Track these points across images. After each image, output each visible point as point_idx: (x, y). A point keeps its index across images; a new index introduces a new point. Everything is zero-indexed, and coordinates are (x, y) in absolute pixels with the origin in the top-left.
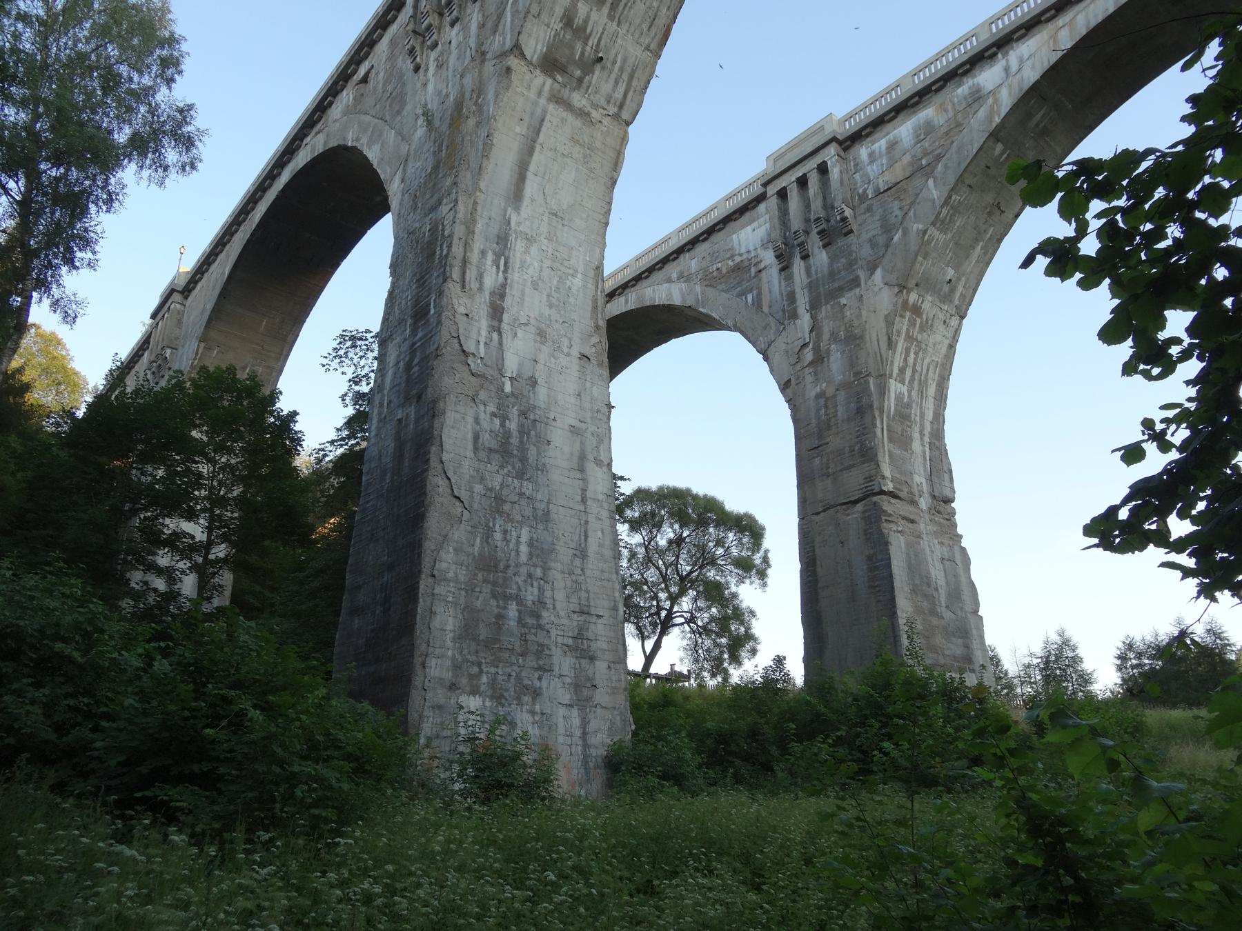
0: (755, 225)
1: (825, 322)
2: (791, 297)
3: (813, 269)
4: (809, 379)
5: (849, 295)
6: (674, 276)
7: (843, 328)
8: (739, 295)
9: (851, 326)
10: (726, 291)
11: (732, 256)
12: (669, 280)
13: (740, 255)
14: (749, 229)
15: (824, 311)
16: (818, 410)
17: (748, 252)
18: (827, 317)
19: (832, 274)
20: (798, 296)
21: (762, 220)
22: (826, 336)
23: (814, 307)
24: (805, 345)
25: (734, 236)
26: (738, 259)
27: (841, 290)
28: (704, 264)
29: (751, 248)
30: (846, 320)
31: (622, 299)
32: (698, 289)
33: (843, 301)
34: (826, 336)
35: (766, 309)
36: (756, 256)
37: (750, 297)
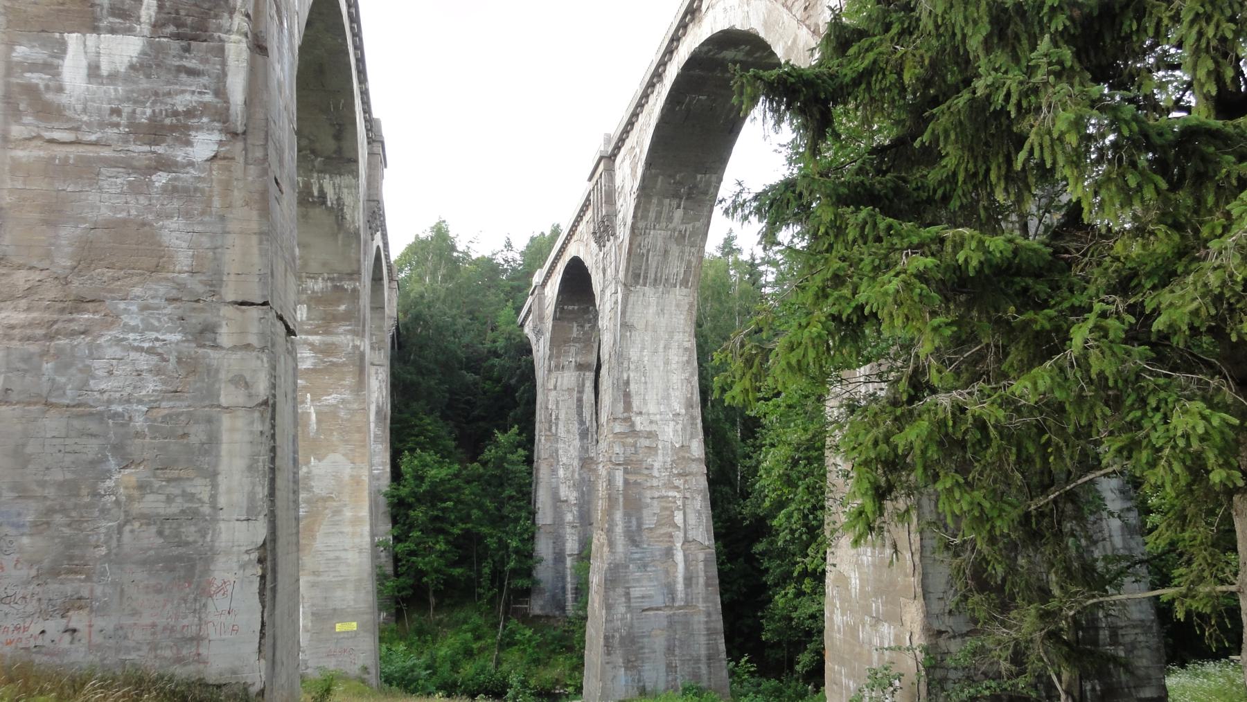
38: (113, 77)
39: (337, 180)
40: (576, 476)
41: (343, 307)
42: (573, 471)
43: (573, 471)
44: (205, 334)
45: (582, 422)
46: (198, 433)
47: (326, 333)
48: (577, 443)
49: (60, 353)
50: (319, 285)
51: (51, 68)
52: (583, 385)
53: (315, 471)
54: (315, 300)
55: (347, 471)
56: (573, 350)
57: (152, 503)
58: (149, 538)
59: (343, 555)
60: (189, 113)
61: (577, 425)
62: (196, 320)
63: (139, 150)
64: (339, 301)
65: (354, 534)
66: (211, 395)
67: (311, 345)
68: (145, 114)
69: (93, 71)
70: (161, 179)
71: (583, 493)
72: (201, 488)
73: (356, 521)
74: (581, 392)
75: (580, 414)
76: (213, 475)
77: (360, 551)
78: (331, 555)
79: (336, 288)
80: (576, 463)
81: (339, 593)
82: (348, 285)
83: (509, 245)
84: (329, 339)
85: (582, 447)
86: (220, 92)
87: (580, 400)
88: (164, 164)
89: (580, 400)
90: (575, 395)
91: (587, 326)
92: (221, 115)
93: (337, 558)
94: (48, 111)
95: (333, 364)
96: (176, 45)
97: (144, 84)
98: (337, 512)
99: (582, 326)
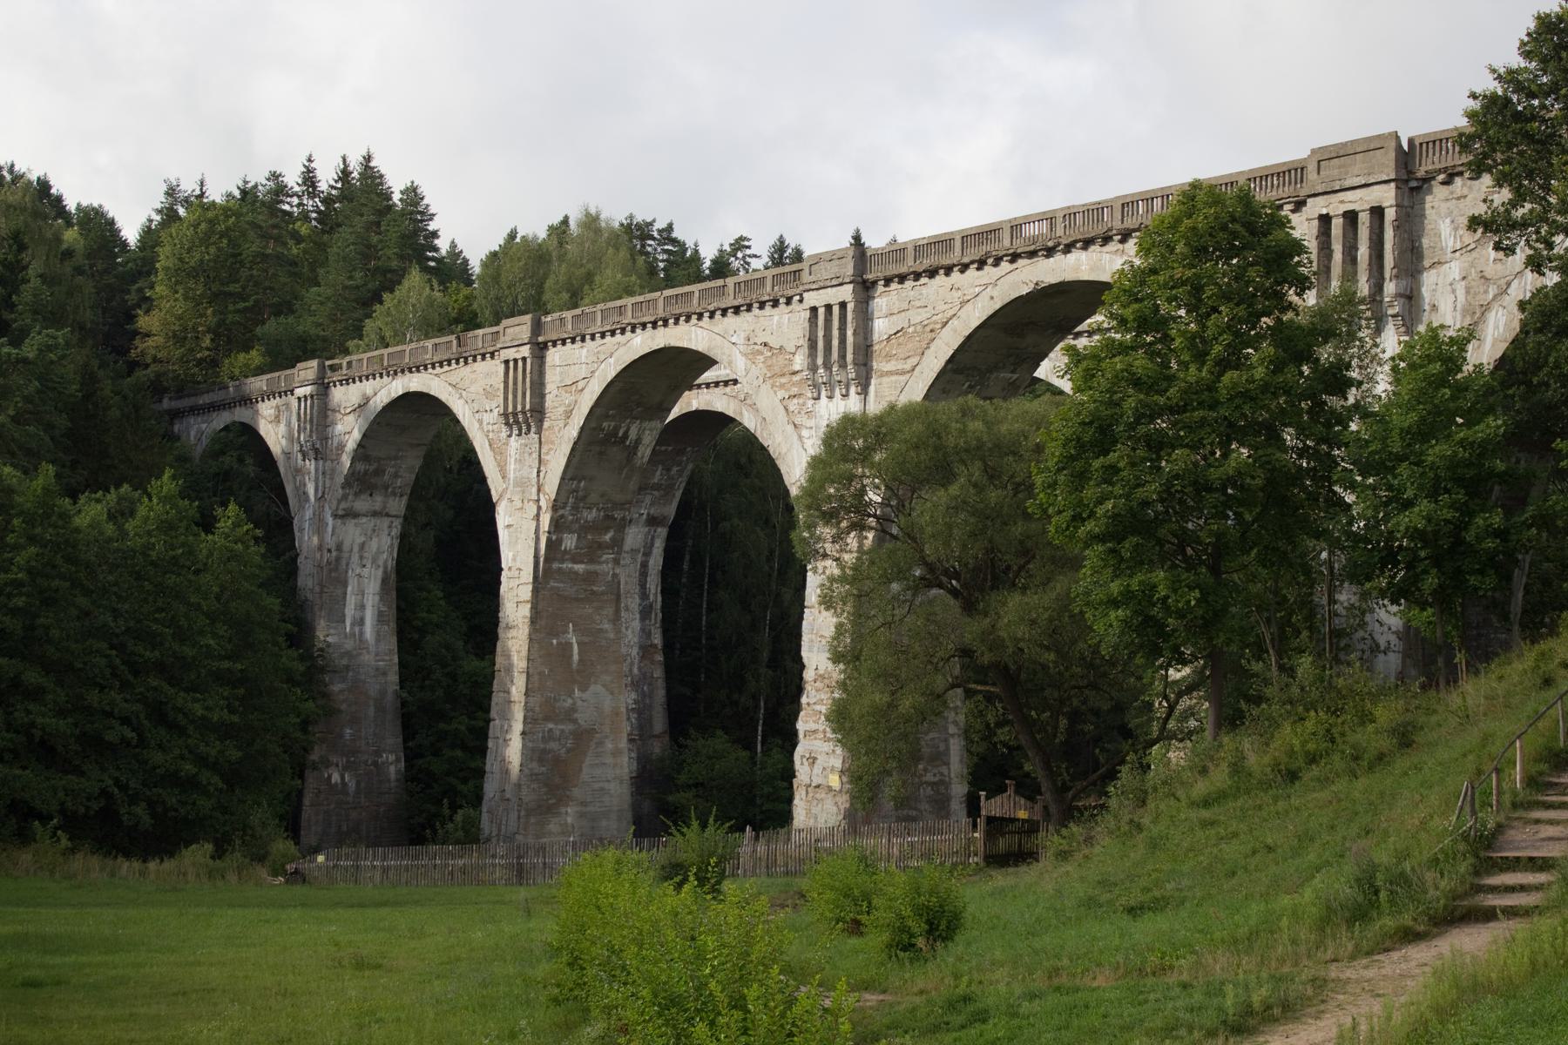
39: (646, 424)
40: (636, 671)
41: (608, 537)
42: (632, 664)
43: (632, 664)
45: (644, 595)
46: (942, 747)
47: (592, 561)
48: (637, 624)
50: (591, 515)
52: (652, 545)
53: (579, 703)
54: (585, 529)
55: (608, 704)
56: (648, 499)
57: (929, 777)
58: (929, 791)
59: (606, 785)
61: (638, 600)
64: (607, 529)
65: (615, 765)
66: (946, 729)
67: (576, 573)
71: (644, 695)
72: (944, 770)
73: (616, 753)
74: (647, 554)
75: (643, 585)
76: (947, 764)
77: (621, 782)
78: (596, 786)
79: (607, 517)
80: (635, 651)
81: (604, 823)
82: (618, 515)
83: (309, 179)
84: (592, 567)
85: (643, 630)
87: (644, 565)
89: (644, 565)
90: (640, 558)
91: (675, 469)
93: (602, 789)
95: (593, 593)
98: (600, 743)
99: (669, 470)
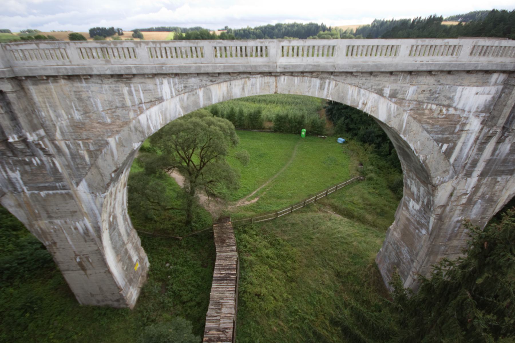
0: (480, 89)
1: (483, 186)
2: (474, 164)
3: (497, 152)
4: (458, 212)
5: (504, 177)
6: (387, 92)
7: (490, 193)
8: (437, 141)
9: (494, 194)
10: (429, 132)
11: (448, 106)
12: (380, 93)
13: (456, 109)
14: (475, 89)
15: (487, 180)
16: (455, 227)
17: (463, 110)
18: (486, 184)
19: (505, 161)
20: (478, 164)
21: (487, 89)
22: (479, 194)
23: (482, 175)
24: (465, 194)
25: (460, 88)
26: (452, 111)
27: (503, 173)
28: (422, 97)
29: (467, 109)
30: (494, 190)
31: (317, 82)
32: (405, 116)
33: (499, 179)
34: (479, 194)
35: (452, 160)
36: (467, 118)
37: (445, 146)
38: (415, 210)
44: (413, 261)
49: (397, 245)
51: (409, 201)
60: (423, 224)
62: (412, 258)
63: (416, 224)
68: (418, 219)
69: (413, 207)
70: (417, 231)
76: (405, 281)
86: (428, 224)
88: (418, 229)
92: (427, 229)
94: (407, 209)
96: (423, 212)
97: (418, 214)
